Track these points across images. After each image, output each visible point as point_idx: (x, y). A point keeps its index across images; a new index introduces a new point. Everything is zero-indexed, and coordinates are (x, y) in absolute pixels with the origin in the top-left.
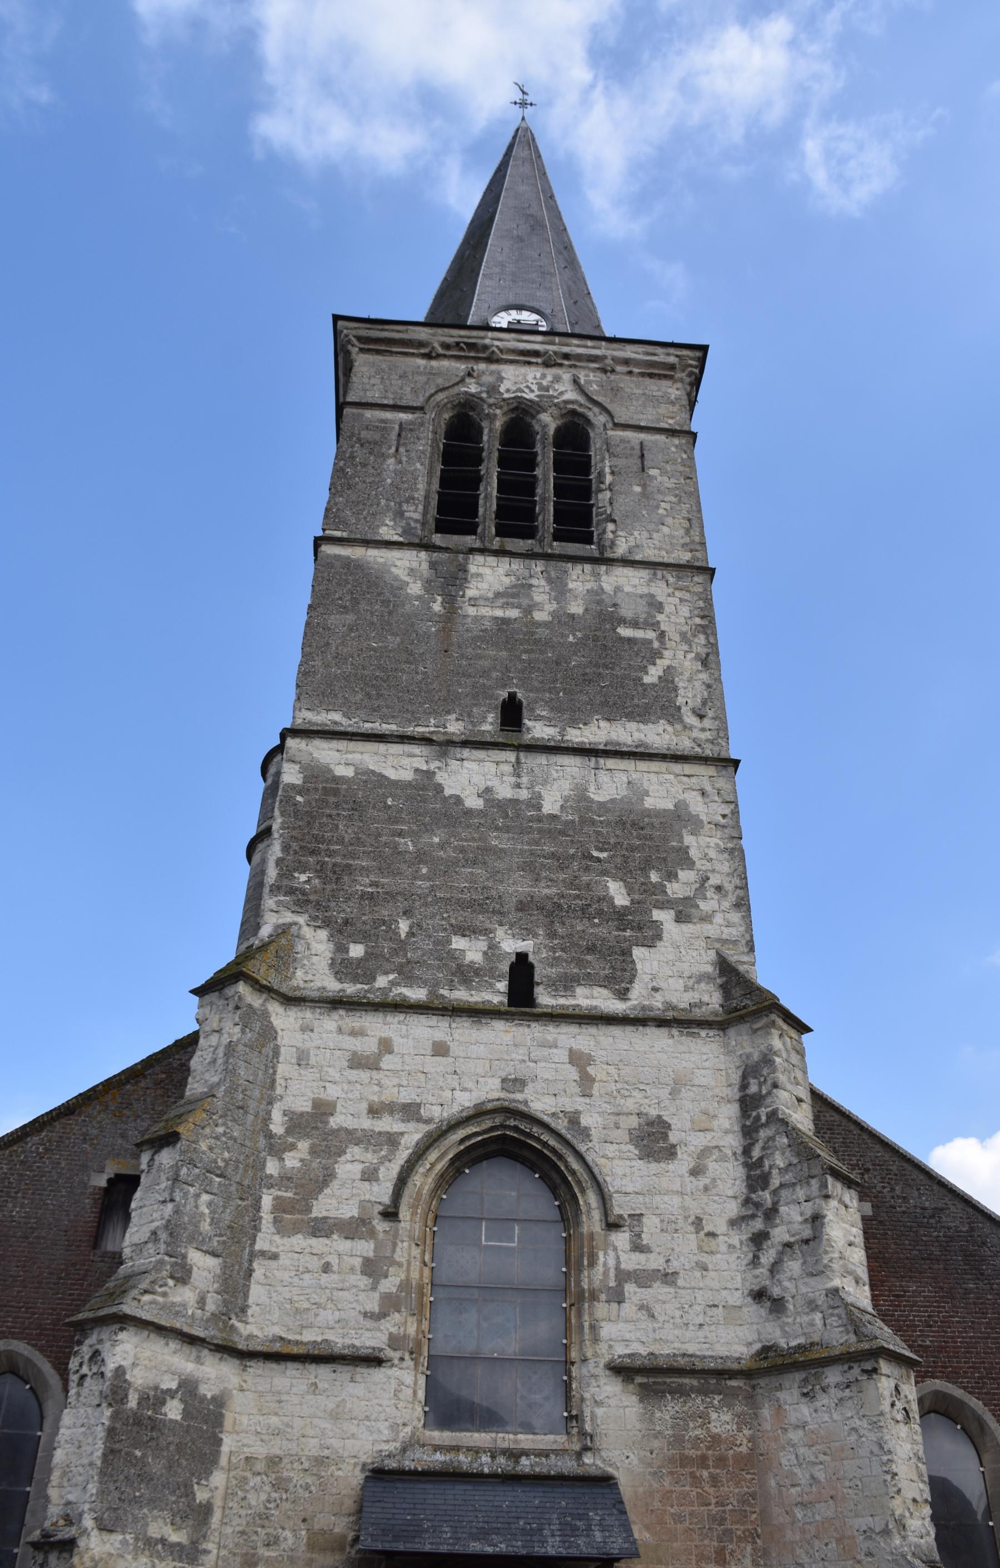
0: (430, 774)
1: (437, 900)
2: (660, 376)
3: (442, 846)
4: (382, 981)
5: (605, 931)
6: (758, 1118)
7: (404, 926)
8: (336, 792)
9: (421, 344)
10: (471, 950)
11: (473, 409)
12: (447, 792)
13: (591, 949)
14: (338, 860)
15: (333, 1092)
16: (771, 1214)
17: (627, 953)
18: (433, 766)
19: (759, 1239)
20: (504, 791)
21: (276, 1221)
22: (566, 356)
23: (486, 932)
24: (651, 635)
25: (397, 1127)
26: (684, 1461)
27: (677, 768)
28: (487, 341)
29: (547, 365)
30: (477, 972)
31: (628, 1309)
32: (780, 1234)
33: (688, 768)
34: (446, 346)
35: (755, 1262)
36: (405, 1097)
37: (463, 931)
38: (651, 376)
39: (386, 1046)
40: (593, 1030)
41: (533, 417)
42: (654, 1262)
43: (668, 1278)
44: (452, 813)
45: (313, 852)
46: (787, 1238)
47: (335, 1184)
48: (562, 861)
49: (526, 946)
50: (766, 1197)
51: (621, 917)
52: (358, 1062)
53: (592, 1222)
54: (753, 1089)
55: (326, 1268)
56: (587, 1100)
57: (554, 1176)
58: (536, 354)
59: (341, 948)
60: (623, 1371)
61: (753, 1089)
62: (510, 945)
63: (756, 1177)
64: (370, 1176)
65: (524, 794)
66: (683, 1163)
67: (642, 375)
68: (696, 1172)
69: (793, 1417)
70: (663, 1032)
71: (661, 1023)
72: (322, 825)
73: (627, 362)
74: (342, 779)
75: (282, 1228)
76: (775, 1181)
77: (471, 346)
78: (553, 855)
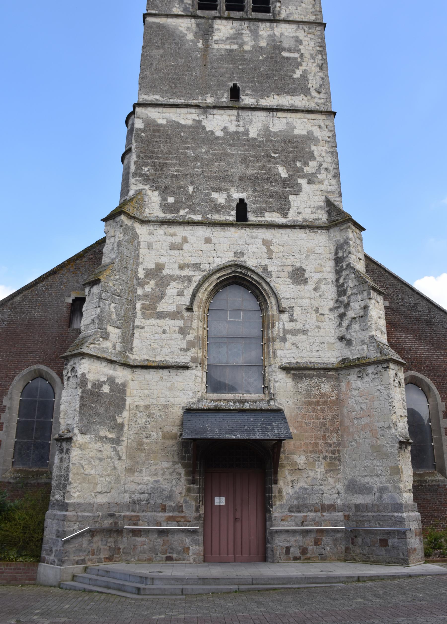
0: (199, 122)
1: (205, 177)
3: (206, 153)
4: (182, 213)
5: (277, 188)
6: (342, 266)
7: (190, 189)
8: (159, 131)
10: (220, 198)
12: (207, 129)
13: (271, 196)
14: (161, 161)
15: (163, 260)
16: (347, 306)
17: (287, 198)
18: (201, 118)
19: (342, 316)
20: (233, 128)
21: (143, 313)
23: (226, 190)
24: (297, 55)
26: (310, 403)
27: (308, 116)
30: (223, 207)
31: (288, 345)
32: (350, 314)
33: (313, 116)
35: (340, 325)
36: (194, 261)
37: (217, 190)
39: (185, 240)
40: (272, 231)
42: (299, 326)
43: (304, 332)
44: (210, 139)
45: (150, 158)
46: (353, 315)
47: (166, 298)
48: (258, 158)
49: (243, 195)
50: (345, 299)
51: (284, 182)
52: (173, 247)
53: (273, 310)
54: (340, 254)
55: (164, 332)
56: (270, 260)
57: (257, 292)
59: (164, 199)
60: (286, 369)
61: (340, 254)
62: (237, 195)
63: (341, 291)
64: (180, 294)
65: (241, 129)
66: (311, 285)
68: (316, 289)
69: (354, 385)
70: (302, 231)
71: (302, 227)
72: (153, 146)
74: (161, 125)
76: (349, 292)
78: (254, 156)
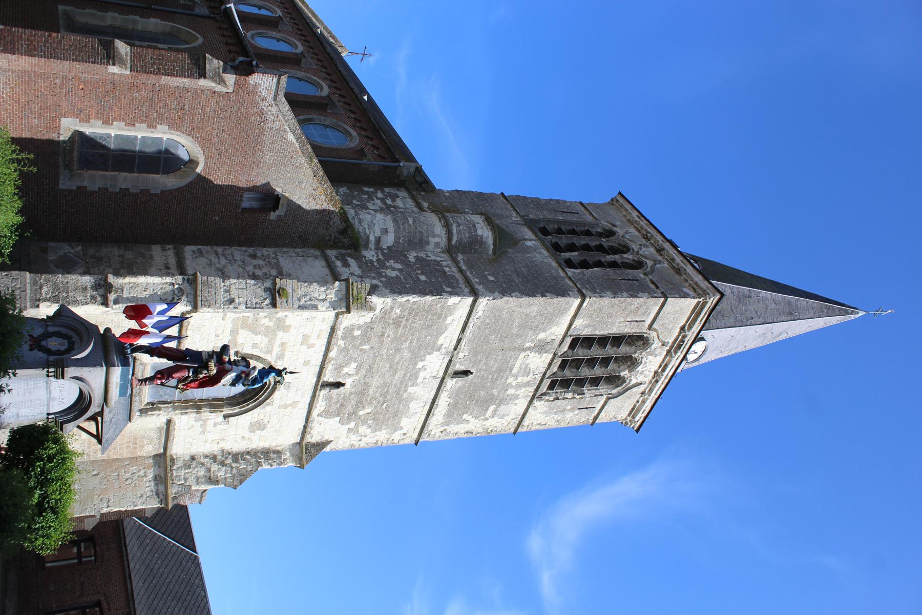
0: (439, 349)
1: (376, 357)
2: (631, 412)
3: (402, 357)
4: (341, 343)
5: (350, 408)
6: (260, 458)
7: (366, 347)
8: (439, 318)
9: (690, 327)
10: (351, 368)
11: (644, 344)
12: (428, 356)
13: (342, 405)
14: (404, 322)
15: (293, 331)
16: (223, 464)
17: (338, 415)
18: (443, 351)
19: (214, 458)
20: (422, 375)
21: (238, 318)
22: (657, 381)
23: (357, 374)
24: (488, 415)
25: (274, 353)
26: (135, 439)
27: (420, 426)
28: (679, 354)
29: (656, 372)
30: (339, 372)
31: (193, 423)
32: (215, 467)
33: (418, 431)
34: (684, 337)
35: (206, 457)
36: (287, 354)
37: (358, 368)
38: (633, 409)
39: (311, 346)
40: (307, 407)
41: (629, 367)
42: (208, 429)
43: (203, 433)
44: (416, 357)
45: (410, 314)
46: (212, 470)
47: (253, 335)
48: (385, 395)
49: (347, 386)
50: (229, 461)
51: (355, 413)
52: (305, 338)
53: (227, 411)
54: (272, 455)
55: (217, 336)
56: (313, 349)
57: (249, 396)
58: (663, 371)
59: (359, 327)
60: (169, 422)
61: (272, 455)
62: (348, 382)
63: (236, 457)
64: (255, 346)
65: (419, 380)
66: (247, 434)
67: (635, 406)
68: (243, 438)
69: (149, 471)
70: (302, 427)
71: (305, 427)
72: (423, 316)
73: (644, 402)
74: (446, 318)
75: (235, 321)
76: (234, 465)
77: (679, 347)
78: (388, 392)
